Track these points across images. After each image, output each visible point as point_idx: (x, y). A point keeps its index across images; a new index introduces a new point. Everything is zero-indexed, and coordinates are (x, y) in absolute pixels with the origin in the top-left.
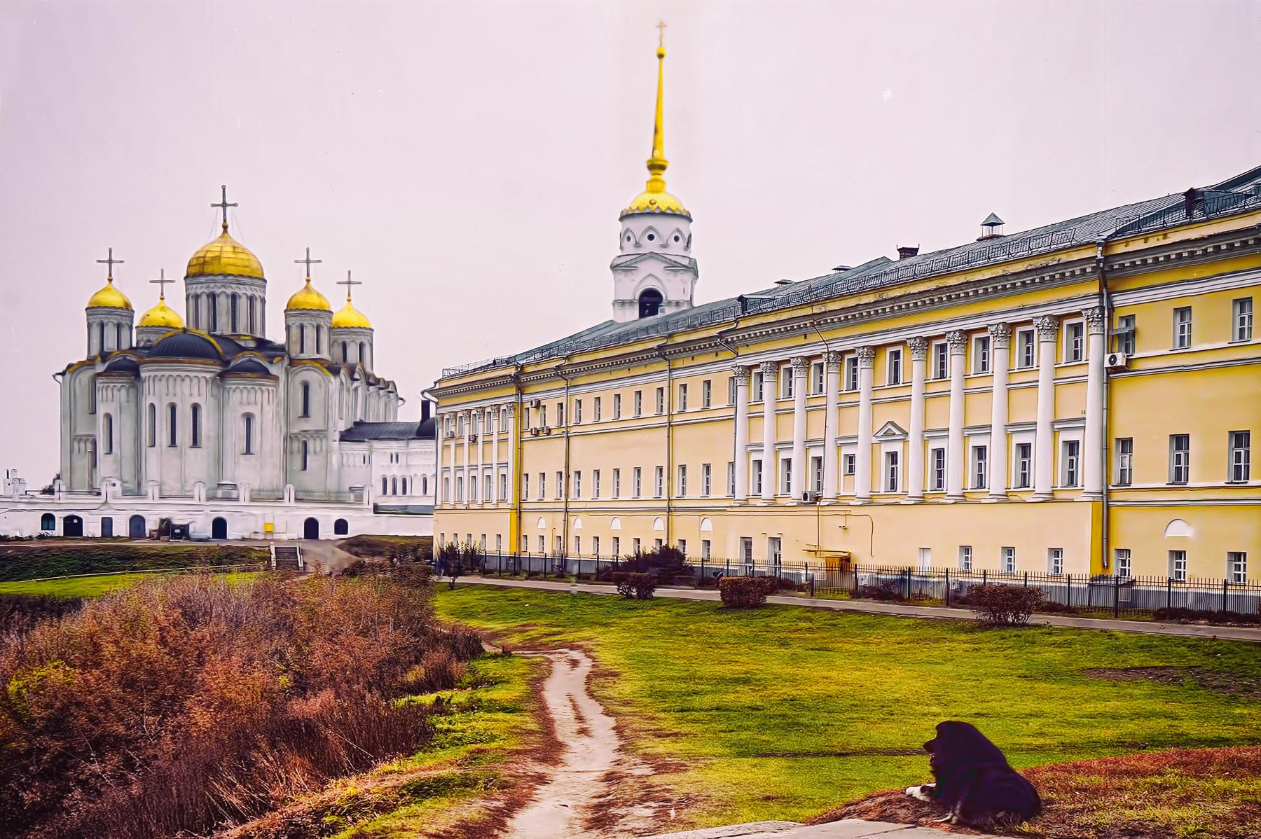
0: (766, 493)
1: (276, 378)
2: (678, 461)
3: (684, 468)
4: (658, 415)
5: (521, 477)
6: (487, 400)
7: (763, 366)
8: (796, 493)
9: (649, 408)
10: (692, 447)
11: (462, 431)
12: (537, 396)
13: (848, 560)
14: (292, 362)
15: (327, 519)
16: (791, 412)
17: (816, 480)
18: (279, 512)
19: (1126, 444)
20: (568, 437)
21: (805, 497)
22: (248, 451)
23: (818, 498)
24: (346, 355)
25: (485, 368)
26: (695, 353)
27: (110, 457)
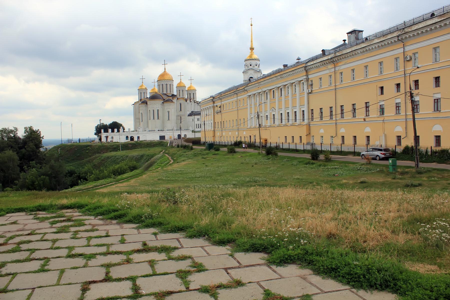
1: (174, 103)
5: (215, 123)
13: (266, 140)
19: (312, 110)
24: (191, 96)
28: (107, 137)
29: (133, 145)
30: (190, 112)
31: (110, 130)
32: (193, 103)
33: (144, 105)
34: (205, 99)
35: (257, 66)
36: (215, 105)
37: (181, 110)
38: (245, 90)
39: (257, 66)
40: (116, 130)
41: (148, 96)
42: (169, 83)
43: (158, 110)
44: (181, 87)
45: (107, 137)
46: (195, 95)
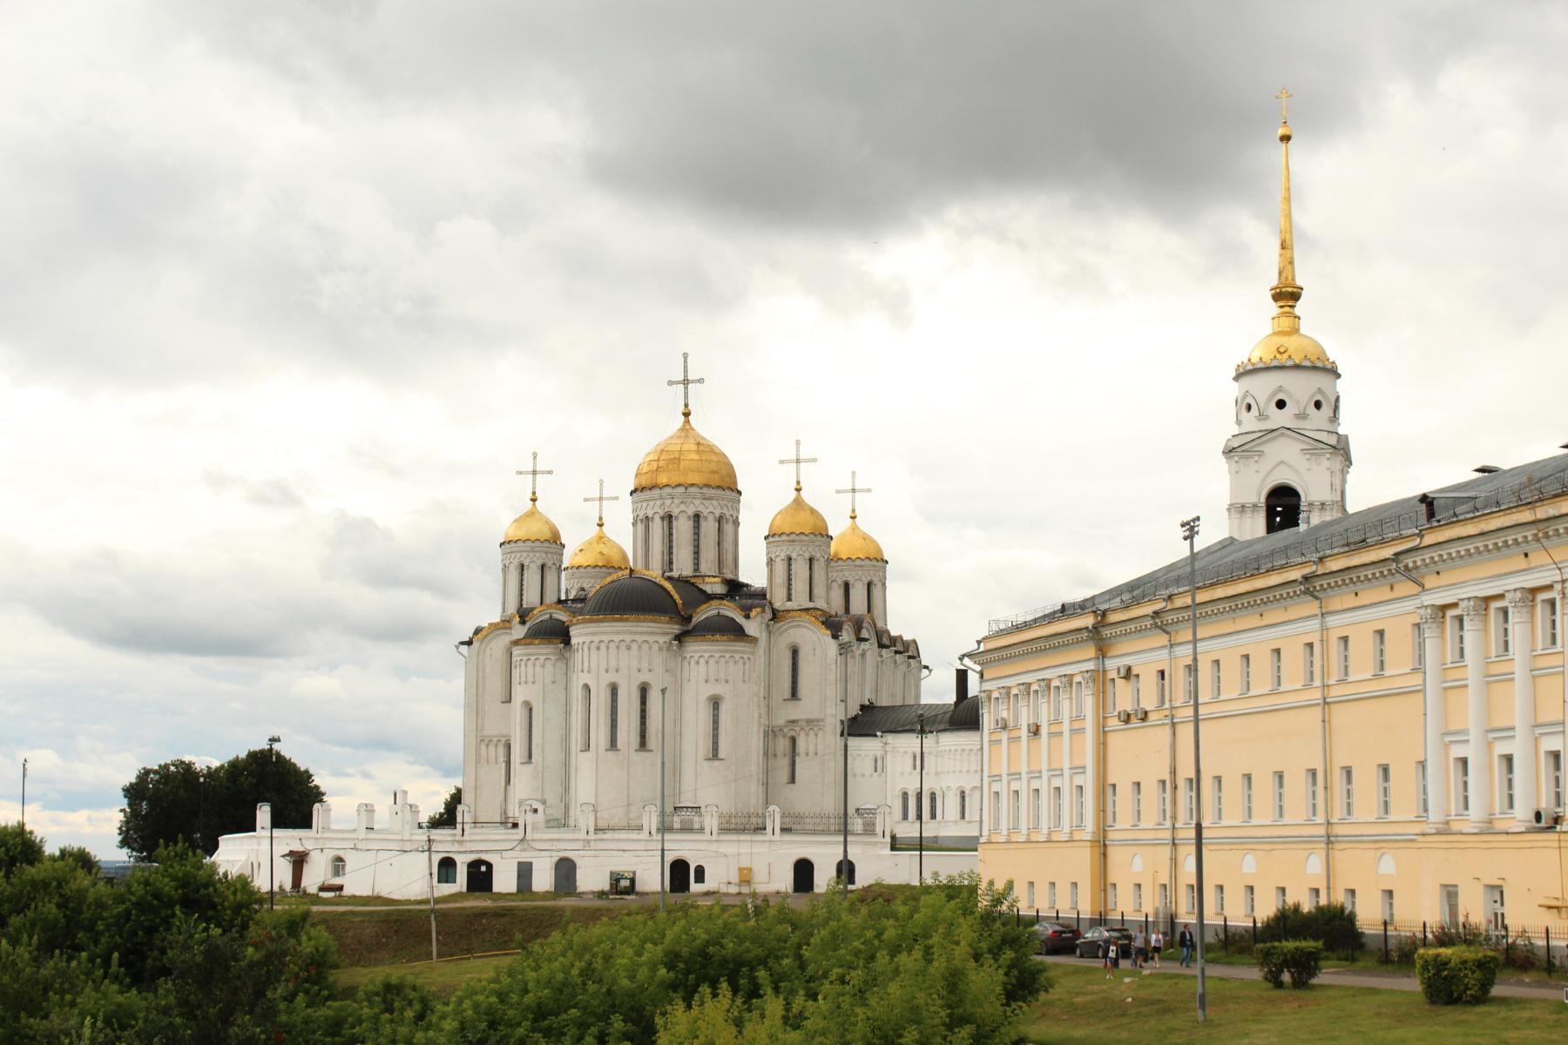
0: (1476, 812)
1: (753, 640)
2: (1340, 760)
3: (1348, 772)
4: (1308, 686)
5: (1105, 788)
6: (1053, 667)
7: (1463, 604)
8: (1522, 814)
10: (1362, 737)
11: (1016, 717)
12: (1127, 661)
16: (1508, 678)
17: (1553, 789)
18: (757, 849)
20: (1173, 725)
21: (1538, 816)
22: (715, 754)
23: (1557, 820)
25: (1050, 618)
26: (1359, 586)
27: (529, 768)
28: (299, 860)
30: (854, 710)
32: (870, 647)
33: (544, 652)
34: (1026, 626)
35: (1326, 410)
36: (1111, 664)
38: (1401, 568)
39: (1326, 410)
42: (710, 509)
43: (644, 690)
45: (299, 860)
46: (876, 592)
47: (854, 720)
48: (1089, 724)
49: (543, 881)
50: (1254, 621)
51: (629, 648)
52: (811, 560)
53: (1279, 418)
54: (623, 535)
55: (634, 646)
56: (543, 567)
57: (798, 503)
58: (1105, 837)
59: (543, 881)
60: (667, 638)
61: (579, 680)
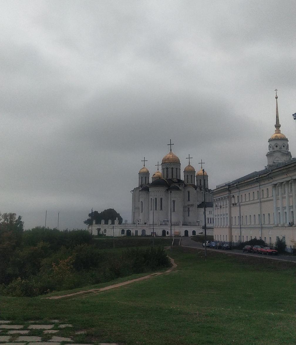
1: (181, 190)
3: (264, 214)
8: (288, 223)
9: (256, 198)
12: (233, 194)
14: (185, 186)
15: (190, 230)
29: (128, 240)
31: (103, 222)
35: (285, 147)
36: (231, 194)
37: (189, 200)
39: (285, 147)
40: (110, 222)
41: (151, 181)
43: (161, 199)
44: (190, 172)
45: (99, 230)
46: (206, 181)
47: (200, 205)
48: (228, 206)
49: (140, 233)
50: (251, 187)
51: (158, 191)
52: (191, 176)
53: (276, 149)
54: (160, 171)
55: (159, 191)
56: (146, 177)
57: (189, 165)
58: (231, 227)
59: (140, 233)
60: (165, 190)
61: (151, 197)
